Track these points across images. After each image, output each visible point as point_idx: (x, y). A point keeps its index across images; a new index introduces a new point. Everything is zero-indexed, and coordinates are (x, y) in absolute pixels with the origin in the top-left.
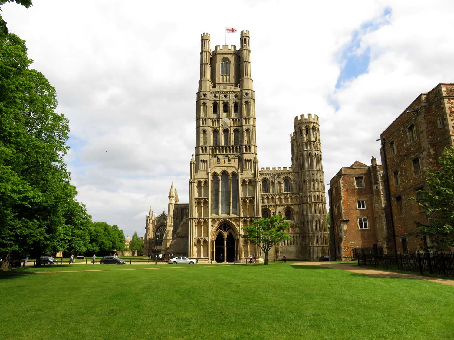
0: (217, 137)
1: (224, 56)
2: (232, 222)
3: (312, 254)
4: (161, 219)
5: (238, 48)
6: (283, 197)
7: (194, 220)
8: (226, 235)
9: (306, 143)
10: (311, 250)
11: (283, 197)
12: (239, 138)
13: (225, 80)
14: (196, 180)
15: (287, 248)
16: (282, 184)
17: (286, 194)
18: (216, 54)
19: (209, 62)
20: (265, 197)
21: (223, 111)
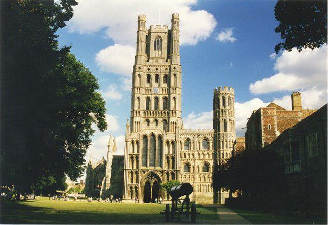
5: (170, 29)
6: (201, 153)
8: (152, 182)
9: (222, 110)
11: (201, 153)
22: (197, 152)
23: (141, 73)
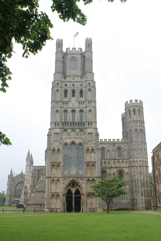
0: (67, 116)
1: (73, 55)
2: (79, 181)
3: (138, 205)
4: (19, 177)
5: (83, 50)
7: (49, 178)
8: (73, 190)
10: (138, 202)
12: (84, 117)
13: (74, 73)
14: (52, 148)
15: (120, 200)
16: (116, 152)
17: (119, 159)
18: (67, 54)
19: (61, 59)
20: (103, 161)
21: (71, 96)
22: (113, 161)
23: (59, 88)
